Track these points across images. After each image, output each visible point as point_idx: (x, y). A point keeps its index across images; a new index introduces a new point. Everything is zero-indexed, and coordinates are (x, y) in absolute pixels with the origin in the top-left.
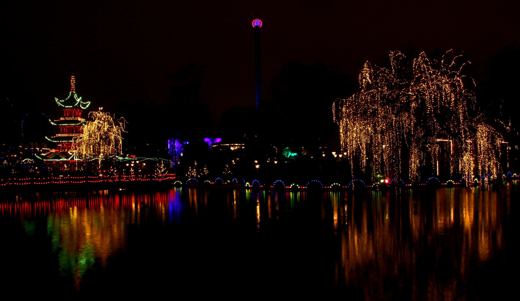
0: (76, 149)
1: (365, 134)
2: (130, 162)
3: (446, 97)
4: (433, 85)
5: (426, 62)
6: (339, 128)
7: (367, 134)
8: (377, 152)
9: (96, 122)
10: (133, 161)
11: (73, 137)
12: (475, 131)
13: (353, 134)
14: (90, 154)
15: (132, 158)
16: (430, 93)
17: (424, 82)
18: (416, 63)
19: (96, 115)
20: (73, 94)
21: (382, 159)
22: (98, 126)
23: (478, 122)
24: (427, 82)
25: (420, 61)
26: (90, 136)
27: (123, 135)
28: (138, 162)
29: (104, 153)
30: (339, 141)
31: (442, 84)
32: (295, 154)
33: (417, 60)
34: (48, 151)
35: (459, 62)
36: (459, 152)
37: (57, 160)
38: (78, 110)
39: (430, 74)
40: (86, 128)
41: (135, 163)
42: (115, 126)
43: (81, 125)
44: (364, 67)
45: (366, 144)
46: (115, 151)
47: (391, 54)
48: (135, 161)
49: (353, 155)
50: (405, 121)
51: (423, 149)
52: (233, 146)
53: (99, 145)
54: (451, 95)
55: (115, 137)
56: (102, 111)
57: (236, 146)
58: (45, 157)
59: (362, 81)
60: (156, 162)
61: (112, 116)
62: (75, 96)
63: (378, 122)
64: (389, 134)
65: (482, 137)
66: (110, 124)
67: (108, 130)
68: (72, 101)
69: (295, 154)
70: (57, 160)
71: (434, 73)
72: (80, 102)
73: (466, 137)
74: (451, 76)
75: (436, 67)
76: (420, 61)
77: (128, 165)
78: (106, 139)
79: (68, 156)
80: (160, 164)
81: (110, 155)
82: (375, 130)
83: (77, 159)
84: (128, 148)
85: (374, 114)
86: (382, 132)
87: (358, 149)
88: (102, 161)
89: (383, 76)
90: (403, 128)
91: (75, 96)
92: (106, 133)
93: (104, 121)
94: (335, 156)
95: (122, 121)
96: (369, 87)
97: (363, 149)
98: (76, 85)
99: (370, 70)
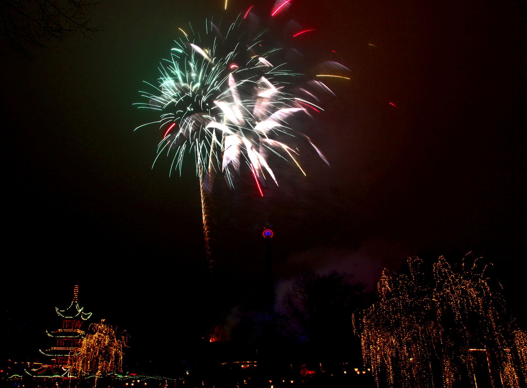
0: (71, 365)
1: (389, 346)
2: (130, 381)
3: (473, 301)
4: (457, 289)
5: (446, 266)
6: (360, 342)
7: (391, 346)
8: (404, 366)
9: (96, 335)
10: (133, 379)
11: (70, 350)
12: (513, 337)
13: (377, 348)
14: (86, 372)
15: (133, 376)
16: (455, 298)
17: (447, 287)
18: (436, 267)
19: (98, 327)
20: (74, 304)
21: (411, 375)
22: (98, 339)
23: (514, 327)
24: (451, 287)
25: (440, 263)
26: (88, 350)
27: (124, 349)
28: (139, 381)
29: (101, 370)
30: (362, 356)
31: (466, 288)
32: (313, 372)
33: (436, 264)
34: (40, 366)
35: (480, 264)
36: (498, 364)
37: (49, 377)
38: (79, 322)
39: (452, 278)
40: (85, 341)
41: (136, 383)
42: (117, 340)
43: (80, 336)
44: (382, 275)
45: (392, 358)
46: (114, 369)
47: (409, 259)
48: (136, 380)
49: (378, 371)
50: (432, 330)
51: (456, 362)
52: (243, 364)
53: (98, 360)
54: (478, 300)
55: (116, 352)
56: (103, 323)
57: (248, 363)
58: (35, 373)
59: (381, 289)
60: (158, 381)
61: (114, 329)
62: (77, 306)
63: (403, 332)
64: (416, 346)
65: (521, 344)
66: (111, 338)
67: (108, 344)
68: (74, 311)
69: (313, 372)
70: (49, 377)
71: (456, 277)
72: (81, 313)
73: (502, 345)
74: (475, 279)
75: (457, 270)
76: (440, 263)
77: (127, 384)
78: (105, 353)
79: (61, 372)
80: (164, 384)
81: (108, 373)
82: (400, 342)
83: (71, 377)
84: (129, 365)
85: (397, 324)
86: (409, 345)
87: (383, 366)
88: (98, 379)
89: (403, 283)
90: (431, 338)
91: (77, 306)
92: (106, 347)
93: (105, 334)
94: (358, 373)
95: (124, 335)
96: (389, 295)
97: (389, 364)
98: (78, 294)
99: (389, 277)
